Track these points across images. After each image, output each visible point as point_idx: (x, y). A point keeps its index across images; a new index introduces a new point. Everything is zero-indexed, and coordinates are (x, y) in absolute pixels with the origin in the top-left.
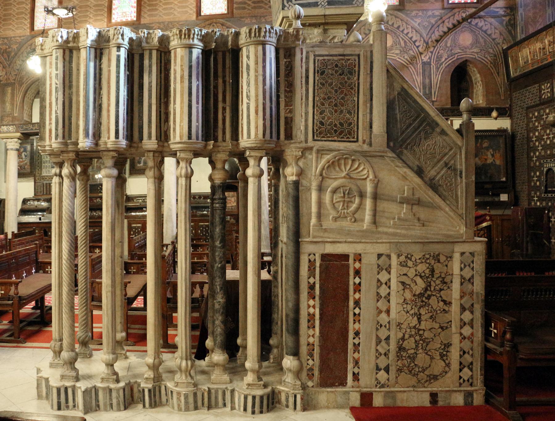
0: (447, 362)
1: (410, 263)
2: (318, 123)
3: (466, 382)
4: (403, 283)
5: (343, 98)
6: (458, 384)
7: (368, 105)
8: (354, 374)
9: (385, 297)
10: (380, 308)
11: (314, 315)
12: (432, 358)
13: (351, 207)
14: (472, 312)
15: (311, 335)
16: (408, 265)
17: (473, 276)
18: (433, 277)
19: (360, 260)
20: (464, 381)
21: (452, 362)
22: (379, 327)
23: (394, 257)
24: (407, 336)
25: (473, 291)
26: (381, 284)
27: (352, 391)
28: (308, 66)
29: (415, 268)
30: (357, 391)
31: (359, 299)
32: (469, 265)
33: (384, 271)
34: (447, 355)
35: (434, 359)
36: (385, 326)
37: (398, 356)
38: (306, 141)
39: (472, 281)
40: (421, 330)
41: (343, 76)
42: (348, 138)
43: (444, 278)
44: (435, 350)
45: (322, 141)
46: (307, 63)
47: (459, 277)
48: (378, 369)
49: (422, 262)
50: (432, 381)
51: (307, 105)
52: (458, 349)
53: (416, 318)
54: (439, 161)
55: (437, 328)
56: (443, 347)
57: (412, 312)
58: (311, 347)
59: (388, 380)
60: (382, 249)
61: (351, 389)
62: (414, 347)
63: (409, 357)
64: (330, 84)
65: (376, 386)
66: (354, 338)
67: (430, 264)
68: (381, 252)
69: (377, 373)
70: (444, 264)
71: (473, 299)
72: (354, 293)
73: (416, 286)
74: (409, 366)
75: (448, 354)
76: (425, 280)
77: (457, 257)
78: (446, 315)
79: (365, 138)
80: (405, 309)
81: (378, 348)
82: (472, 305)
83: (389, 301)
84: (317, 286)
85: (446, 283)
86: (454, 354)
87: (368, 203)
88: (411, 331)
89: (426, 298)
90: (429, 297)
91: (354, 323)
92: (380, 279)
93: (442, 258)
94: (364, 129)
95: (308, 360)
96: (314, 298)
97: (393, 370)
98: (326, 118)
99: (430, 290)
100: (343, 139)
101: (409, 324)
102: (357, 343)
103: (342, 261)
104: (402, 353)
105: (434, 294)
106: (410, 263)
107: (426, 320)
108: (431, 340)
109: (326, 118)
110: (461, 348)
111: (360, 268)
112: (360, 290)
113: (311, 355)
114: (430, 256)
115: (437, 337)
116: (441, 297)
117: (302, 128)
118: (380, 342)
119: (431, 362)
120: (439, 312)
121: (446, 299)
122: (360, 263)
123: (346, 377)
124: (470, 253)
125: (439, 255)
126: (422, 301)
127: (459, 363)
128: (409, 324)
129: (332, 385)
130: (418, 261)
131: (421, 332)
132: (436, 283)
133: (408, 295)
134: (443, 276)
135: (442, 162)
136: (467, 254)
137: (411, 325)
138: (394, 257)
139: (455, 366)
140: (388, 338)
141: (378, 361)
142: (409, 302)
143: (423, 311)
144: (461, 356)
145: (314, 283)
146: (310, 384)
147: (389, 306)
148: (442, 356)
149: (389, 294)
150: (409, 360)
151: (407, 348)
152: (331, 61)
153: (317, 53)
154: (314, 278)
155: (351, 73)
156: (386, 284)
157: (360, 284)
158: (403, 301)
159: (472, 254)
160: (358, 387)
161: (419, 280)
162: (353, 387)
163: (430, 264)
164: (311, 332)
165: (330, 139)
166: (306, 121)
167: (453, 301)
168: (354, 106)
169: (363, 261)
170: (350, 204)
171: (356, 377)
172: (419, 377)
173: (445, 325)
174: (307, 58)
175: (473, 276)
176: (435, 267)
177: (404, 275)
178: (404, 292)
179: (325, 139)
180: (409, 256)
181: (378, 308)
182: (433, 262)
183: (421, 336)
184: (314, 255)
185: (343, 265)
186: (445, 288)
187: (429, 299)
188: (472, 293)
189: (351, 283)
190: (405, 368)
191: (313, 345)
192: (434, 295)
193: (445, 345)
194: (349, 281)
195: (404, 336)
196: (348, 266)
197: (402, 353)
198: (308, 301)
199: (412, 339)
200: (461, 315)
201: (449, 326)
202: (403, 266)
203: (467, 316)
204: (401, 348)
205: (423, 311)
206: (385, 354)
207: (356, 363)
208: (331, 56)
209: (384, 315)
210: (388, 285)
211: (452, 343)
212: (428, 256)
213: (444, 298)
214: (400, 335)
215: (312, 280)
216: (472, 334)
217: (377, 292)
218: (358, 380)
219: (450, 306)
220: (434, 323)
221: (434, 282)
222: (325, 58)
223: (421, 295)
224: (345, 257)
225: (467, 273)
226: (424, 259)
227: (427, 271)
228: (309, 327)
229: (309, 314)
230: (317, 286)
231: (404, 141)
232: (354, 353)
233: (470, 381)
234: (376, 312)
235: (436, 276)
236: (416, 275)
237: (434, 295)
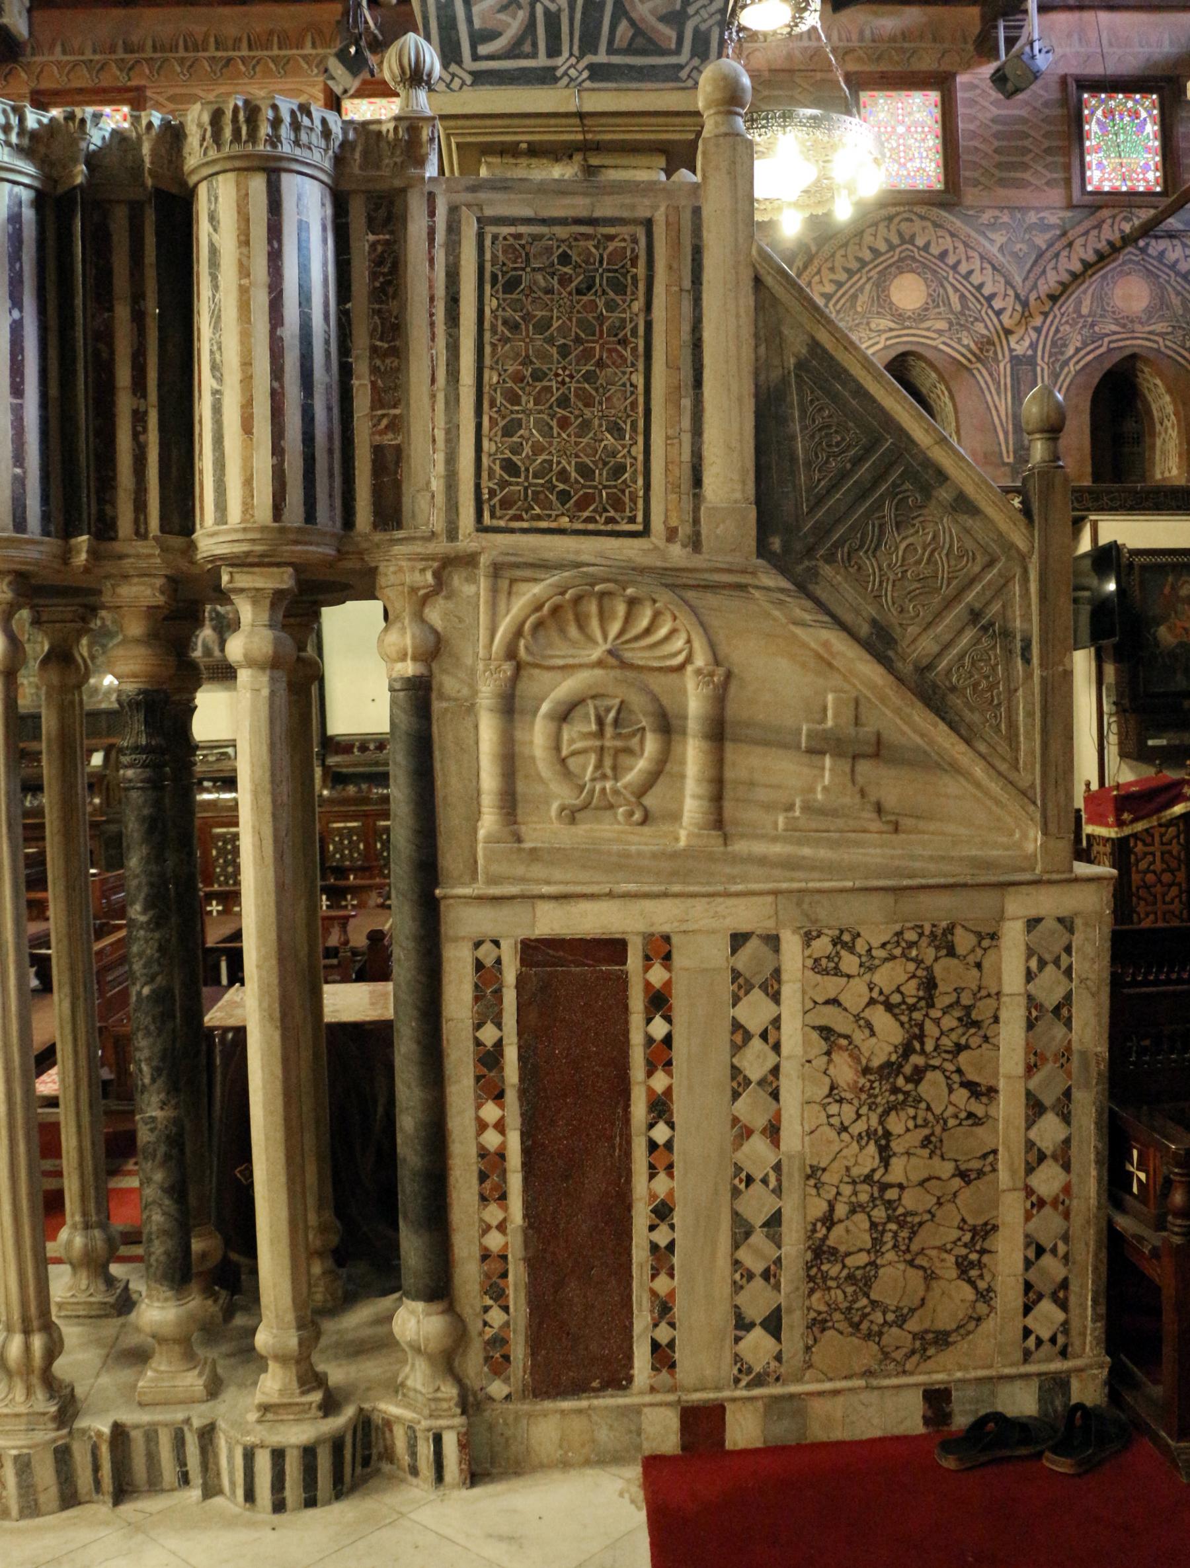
0: (982, 1285)
1: (849, 963)
2: (497, 468)
3: (1047, 1347)
4: (826, 1032)
5: (589, 377)
6: (1019, 1355)
7: (687, 403)
8: (655, 1346)
9: (761, 1083)
10: (745, 1118)
11: (501, 1155)
12: (930, 1277)
13: (631, 769)
14: (1066, 1119)
15: (494, 1223)
16: (844, 967)
17: (1068, 997)
18: (931, 1005)
19: (667, 958)
20: (1039, 1342)
21: (998, 1288)
22: (742, 1186)
23: (791, 945)
24: (841, 1210)
25: (1068, 1048)
26: (748, 1036)
27: (651, 1405)
28: (458, 257)
29: (867, 977)
30: (668, 1404)
31: (669, 1091)
32: (1057, 962)
33: (757, 994)
34: (980, 1265)
35: (938, 1278)
36: (765, 1181)
37: (811, 1279)
38: (452, 534)
39: (1065, 1012)
40: (891, 1186)
41: (589, 297)
42: (610, 520)
43: (968, 1009)
44: (942, 1249)
45: (512, 531)
46: (453, 246)
47: (1023, 1001)
48: (743, 1325)
49: (895, 958)
50: (931, 1351)
51: (453, 402)
52: (1021, 1240)
53: (872, 1149)
54: (949, 604)
55: (944, 1176)
56: (967, 1237)
57: (860, 1127)
58: (496, 1266)
59: (778, 1358)
60: (747, 915)
61: (648, 1399)
62: (869, 1245)
63: (851, 1278)
64: (543, 326)
65: (737, 1381)
66: (652, 1228)
67: (918, 962)
68: (744, 927)
69: (737, 1340)
70: (971, 959)
71: (1069, 1075)
72: (650, 1074)
73: (873, 1040)
74: (849, 1309)
75: (985, 1259)
76: (905, 1019)
77: (1013, 935)
78: (979, 1130)
79: (674, 522)
80: (835, 1121)
81: (743, 1254)
82: (1067, 1093)
83: (775, 1095)
84: (511, 1054)
85: (976, 1024)
86: (1007, 1259)
87: (693, 755)
88: (855, 1193)
89: (908, 1080)
90: (917, 1076)
91: (652, 1176)
92: (742, 1021)
93: (963, 941)
94: (673, 487)
95: (486, 1309)
96: (499, 1097)
97: (794, 1324)
98: (527, 450)
99: (923, 1052)
100: (591, 527)
101: (848, 1169)
102: (663, 1243)
103: (600, 961)
104: (824, 1268)
105: (935, 1062)
106: (849, 963)
107: (908, 1153)
108: (927, 1217)
109: (527, 450)
110: (1027, 1236)
111: (668, 984)
112: (669, 1063)
113: (497, 1293)
114: (921, 935)
115: (950, 1206)
116: (959, 1071)
117: (437, 485)
118: (748, 1234)
119: (928, 1288)
120: (952, 1122)
121: (976, 1079)
122: (668, 968)
123: (630, 1357)
124: (1060, 920)
125: (950, 930)
126: (895, 1090)
127: (1021, 1287)
128: (848, 1169)
129: (579, 1388)
130: (879, 953)
131: (891, 1194)
132: (942, 1026)
133: (844, 1071)
134: (966, 1000)
135: (959, 609)
136: (1050, 924)
137: (855, 1172)
138: (791, 945)
139: (1009, 1294)
140: (774, 1221)
141: (741, 1299)
142: (849, 1096)
143: (896, 1124)
144: (1028, 1264)
145: (499, 1044)
146: (498, 1389)
147: (778, 1115)
148: (963, 1267)
149: (775, 1071)
150: (850, 1290)
151: (842, 1249)
152: (544, 242)
153: (489, 212)
154: (499, 1026)
155: (620, 289)
156: (764, 1036)
157: (668, 1040)
158: (826, 1090)
159: (1067, 924)
160: (673, 1389)
161: (880, 1018)
162: (653, 1389)
163: (918, 962)
164: (493, 1214)
165: (543, 525)
166: (451, 459)
167: (1002, 1085)
168: (634, 405)
169: (678, 960)
170: (624, 760)
171: (663, 1356)
172: (885, 1340)
173: (975, 1164)
174: (453, 228)
175: (1068, 997)
176: (938, 970)
177: (827, 1002)
178: (830, 1061)
179: (525, 525)
180: (846, 937)
181: (735, 1120)
182: (929, 954)
183: (889, 1204)
184: (496, 943)
185: (607, 977)
186: (975, 1041)
187: (917, 1082)
188: (1066, 1053)
189: (637, 1038)
190: (837, 1316)
191: (504, 1258)
192: (935, 1068)
193: (974, 1230)
194: (626, 1033)
195: (832, 1208)
196: (622, 982)
197: (824, 1268)
198: (479, 1107)
199: (861, 1220)
200: (1028, 1128)
201: (988, 1169)
202: (825, 972)
203: (1049, 1131)
204: (820, 1252)
205: (896, 1124)
206: (766, 1275)
207: (664, 1309)
208: (544, 221)
209: (758, 1145)
210: (771, 1040)
211: (999, 1222)
212: (911, 936)
213: (972, 1076)
214: (818, 1207)
215: (489, 1034)
216: (1067, 1189)
217: (733, 1067)
218: (672, 1366)
219: (991, 1099)
220: (936, 1160)
221: (937, 1022)
222: (522, 229)
223: (889, 1069)
224: (615, 948)
225: (1050, 987)
226: (900, 946)
227: (911, 988)
228: (483, 1199)
229: (483, 1153)
230: (511, 1054)
231: (823, 531)
232: (653, 1277)
233: (1061, 1340)
234: (730, 1135)
235: (942, 1001)
236: (872, 1002)
237: (935, 1068)
